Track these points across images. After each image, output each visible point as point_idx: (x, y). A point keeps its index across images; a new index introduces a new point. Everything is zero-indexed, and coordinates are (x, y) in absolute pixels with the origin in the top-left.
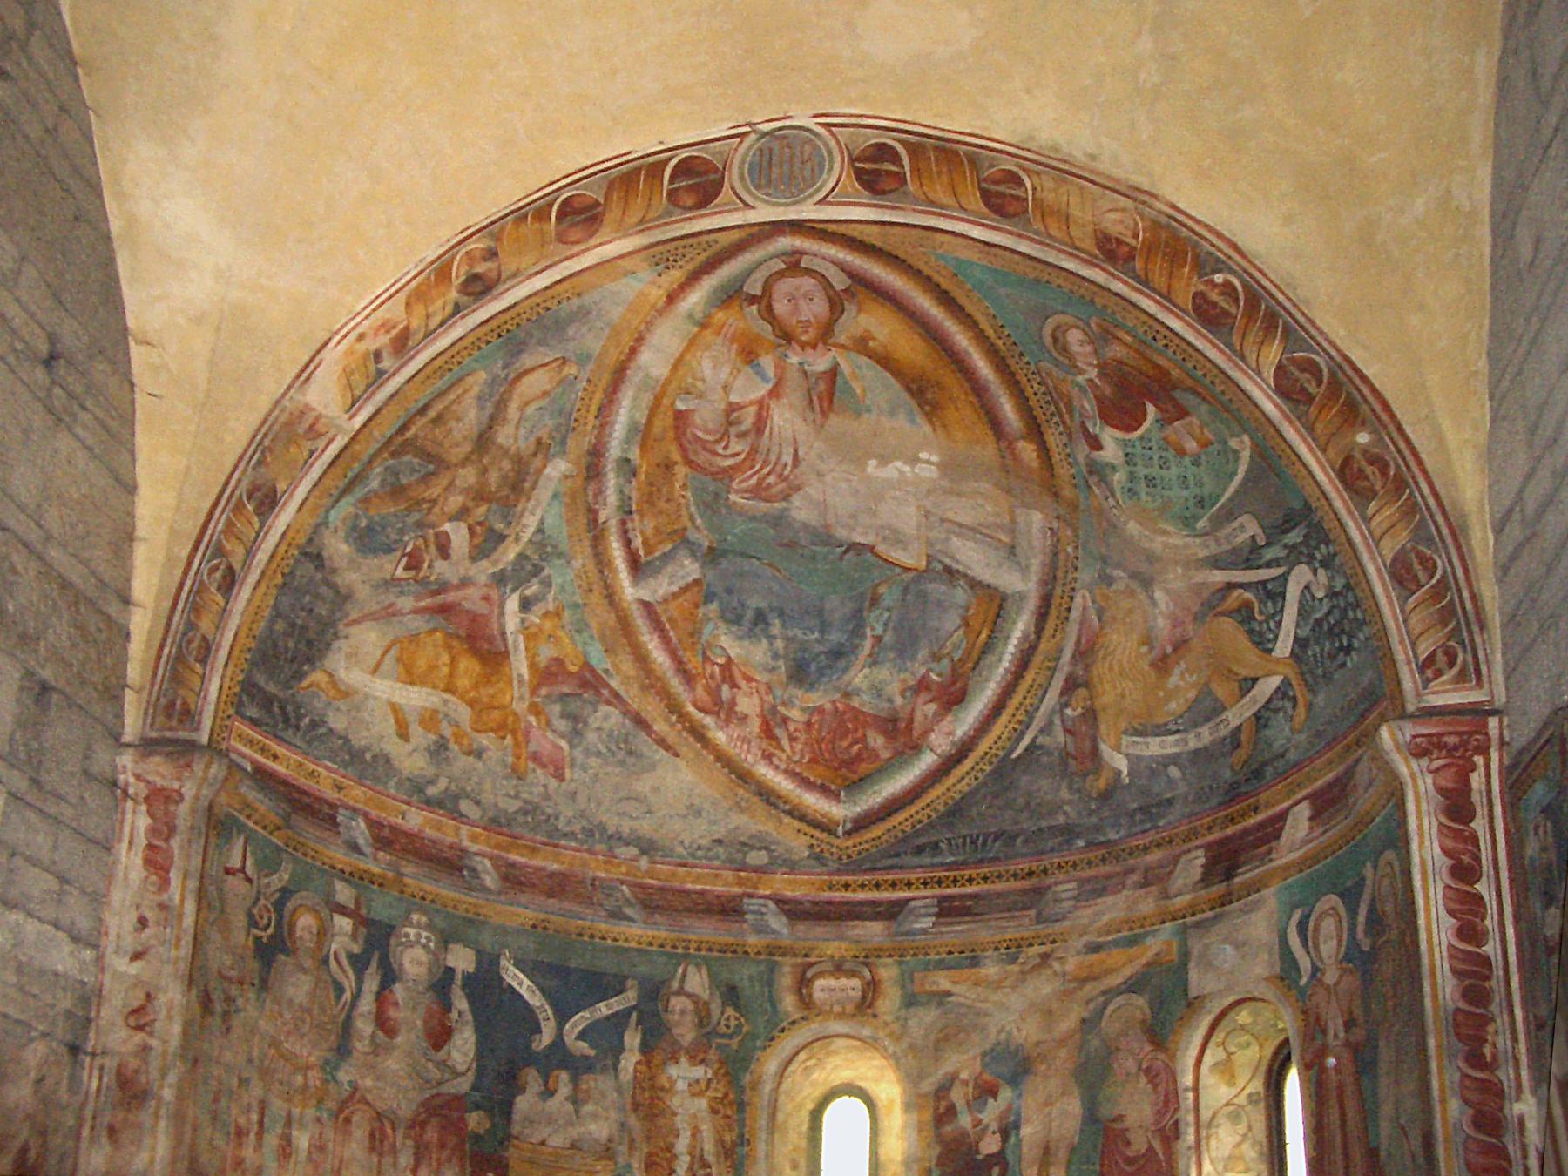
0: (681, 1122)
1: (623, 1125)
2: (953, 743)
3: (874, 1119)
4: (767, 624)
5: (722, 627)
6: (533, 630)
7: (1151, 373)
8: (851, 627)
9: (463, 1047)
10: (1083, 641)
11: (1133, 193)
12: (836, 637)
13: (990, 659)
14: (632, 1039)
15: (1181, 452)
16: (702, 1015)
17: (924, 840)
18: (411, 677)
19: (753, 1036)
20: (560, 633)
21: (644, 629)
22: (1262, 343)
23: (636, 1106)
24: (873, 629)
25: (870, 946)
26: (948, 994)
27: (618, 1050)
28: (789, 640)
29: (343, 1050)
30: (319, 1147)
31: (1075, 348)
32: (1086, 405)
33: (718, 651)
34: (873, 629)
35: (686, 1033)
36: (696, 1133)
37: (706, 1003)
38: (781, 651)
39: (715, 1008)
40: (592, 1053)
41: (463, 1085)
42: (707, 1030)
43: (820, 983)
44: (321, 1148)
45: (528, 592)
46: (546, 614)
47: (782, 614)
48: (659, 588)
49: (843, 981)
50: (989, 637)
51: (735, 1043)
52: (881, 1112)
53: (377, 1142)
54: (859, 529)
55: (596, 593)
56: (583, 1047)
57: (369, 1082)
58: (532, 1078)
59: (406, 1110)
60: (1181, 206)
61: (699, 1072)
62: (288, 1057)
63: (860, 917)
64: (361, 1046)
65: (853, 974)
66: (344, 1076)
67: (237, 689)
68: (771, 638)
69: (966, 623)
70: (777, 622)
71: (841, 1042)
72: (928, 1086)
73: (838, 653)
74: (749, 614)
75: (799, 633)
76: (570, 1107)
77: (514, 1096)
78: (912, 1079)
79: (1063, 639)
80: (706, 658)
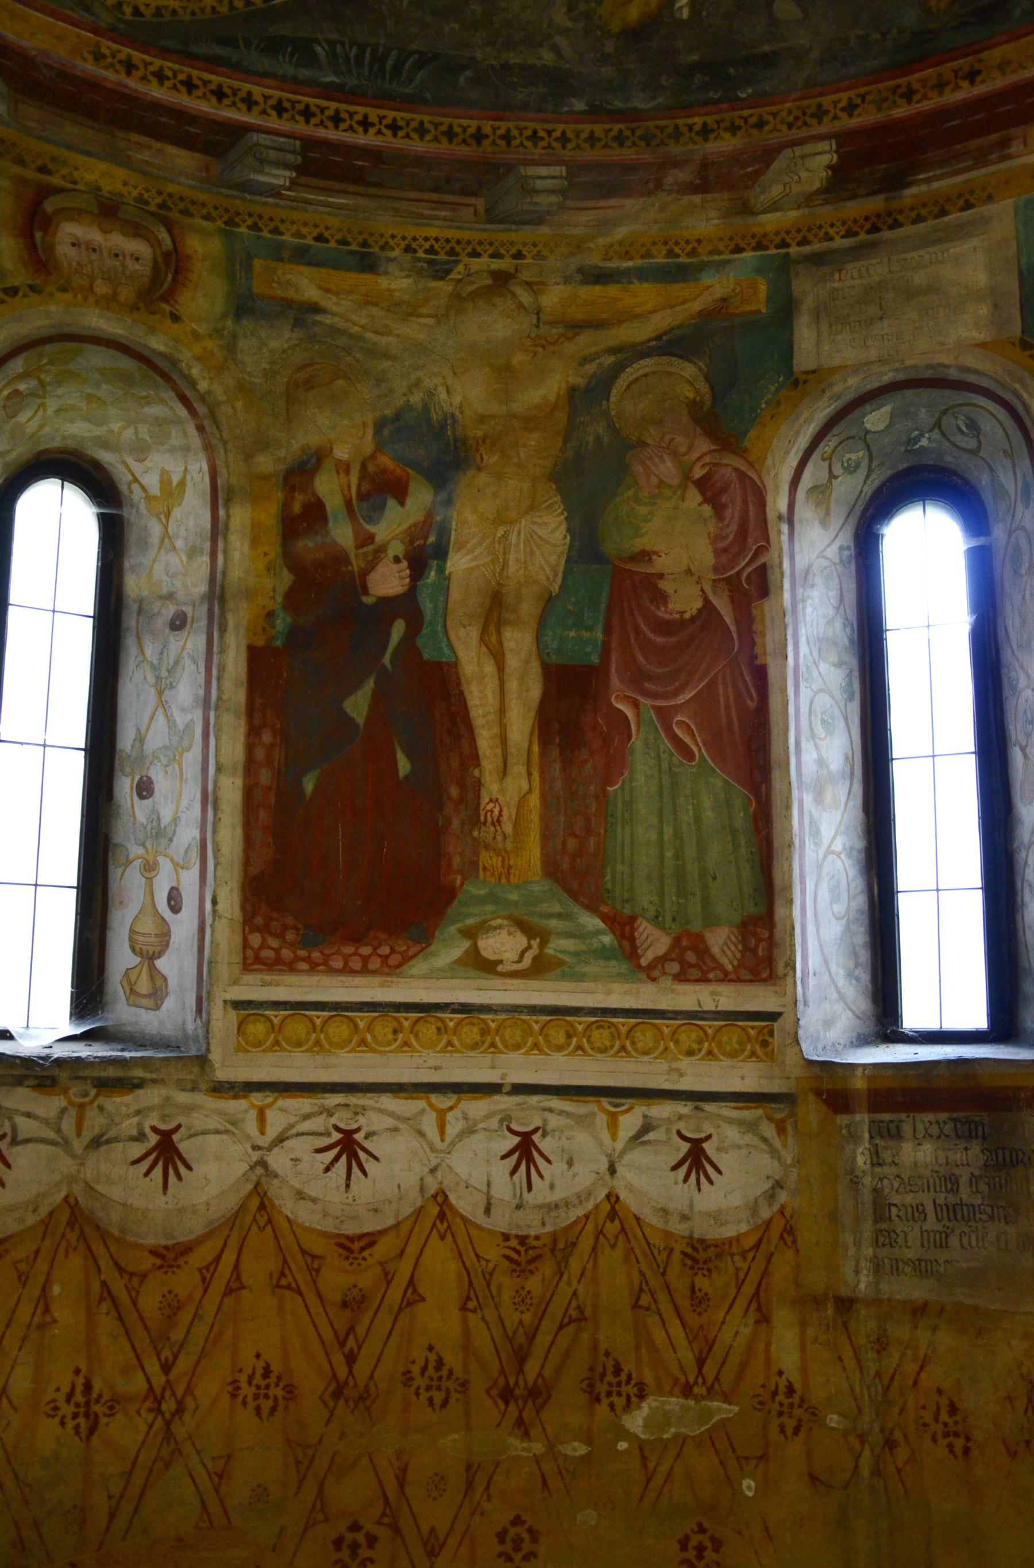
25: (171, 188)
43: (69, 230)
49: (118, 240)
63: (158, 133)
65: (136, 231)
71: (97, 357)
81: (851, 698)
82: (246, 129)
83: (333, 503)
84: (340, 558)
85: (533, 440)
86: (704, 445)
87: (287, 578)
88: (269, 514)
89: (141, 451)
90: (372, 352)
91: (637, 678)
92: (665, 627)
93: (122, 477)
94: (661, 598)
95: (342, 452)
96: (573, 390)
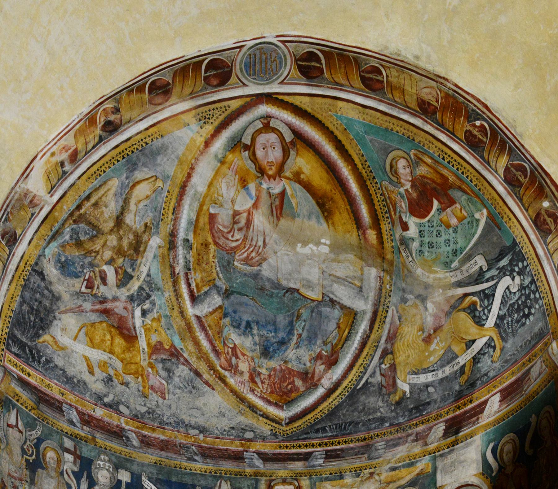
2: (332, 383)
4: (251, 328)
5: (231, 328)
6: (148, 326)
7: (439, 181)
8: (288, 330)
10: (391, 332)
11: (437, 79)
12: (281, 335)
13: (349, 343)
15: (448, 226)
17: (319, 426)
18: (93, 344)
20: (160, 329)
21: (197, 330)
22: (498, 156)
24: (298, 331)
28: (261, 336)
31: (401, 171)
32: (403, 206)
33: (230, 341)
34: (298, 331)
38: (258, 342)
45: (145, 307)
46: (153, 320)
47: (257, 323)
48: (203, 309)
50: (349, 333)
54: (293, 281)
55: (175, 310)
60: (460, 85)
67: (6, 336)
68: (252, 335)
69: (339, 326)
70: (256, 328)
73: (283, 343)
74: (244, 324)
75: (265, 333)
79: (382, 332)
80: (225, 344)
82: (312, 453)
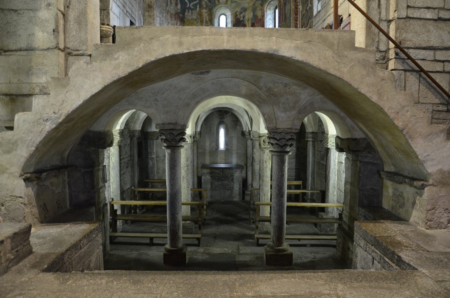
0: (204, 17)
1: (197, 17)
3: (226, 18)
9: (179, 6)
14: (198, 6)
16: (206, 4)
19: (212, 6)
23: (199, 15)
26: (237, 1)
27: (196, 8)
29: (167, 5)
30: (166, 16)
35: (204, 6)
36: (206, 18)
37: (207, 2)
39: (208, 3)
40: (193, 8)
41: (179, 11)
42: (207, 6)
44: (166, 16)
51: (210, 7)
52: (227, 17)
53: (171, 16)
56: (192, 7)
57: (170, 9)
58: (187, 10)
59: (174, 13)
61: (206, 11)
62: (163, 5)
64: (169, 5)
66: (168, 8)
71: (223, 7)
72: (234, 12)
76: (191, 14)
77: (185, 13)
78: (232, 11)
81: (273, 23)
83: (238, 14)
84: (239, 18)
85: (250, 8)
86: (261, 7)
87: (235, 20)
88: (234, 16)
89: (227, 13)
90: (240, 4)
91: (257, 23)
92: (258, 20)
93: (226, 14)
94: (258, 18)
95: (238, 11)
96: (253, 4)
